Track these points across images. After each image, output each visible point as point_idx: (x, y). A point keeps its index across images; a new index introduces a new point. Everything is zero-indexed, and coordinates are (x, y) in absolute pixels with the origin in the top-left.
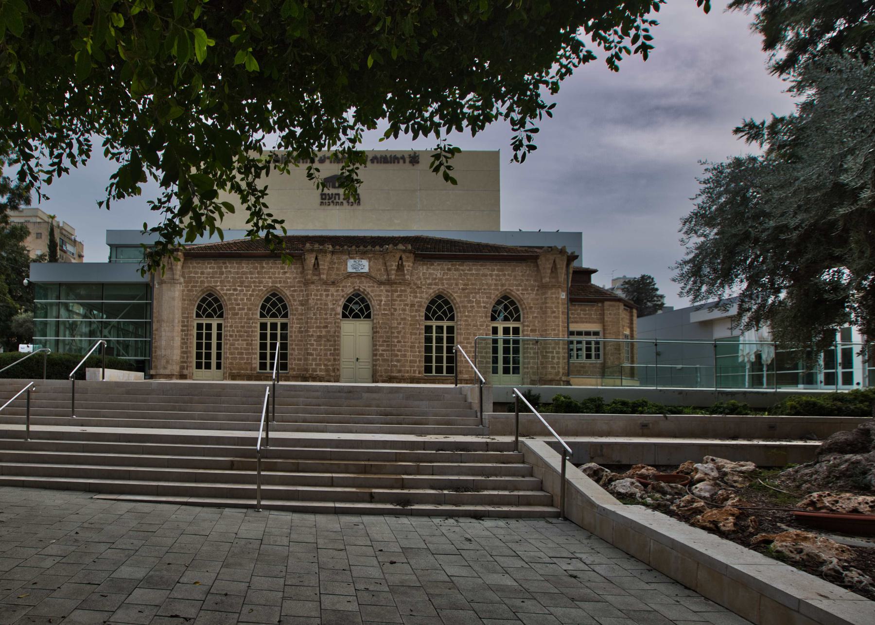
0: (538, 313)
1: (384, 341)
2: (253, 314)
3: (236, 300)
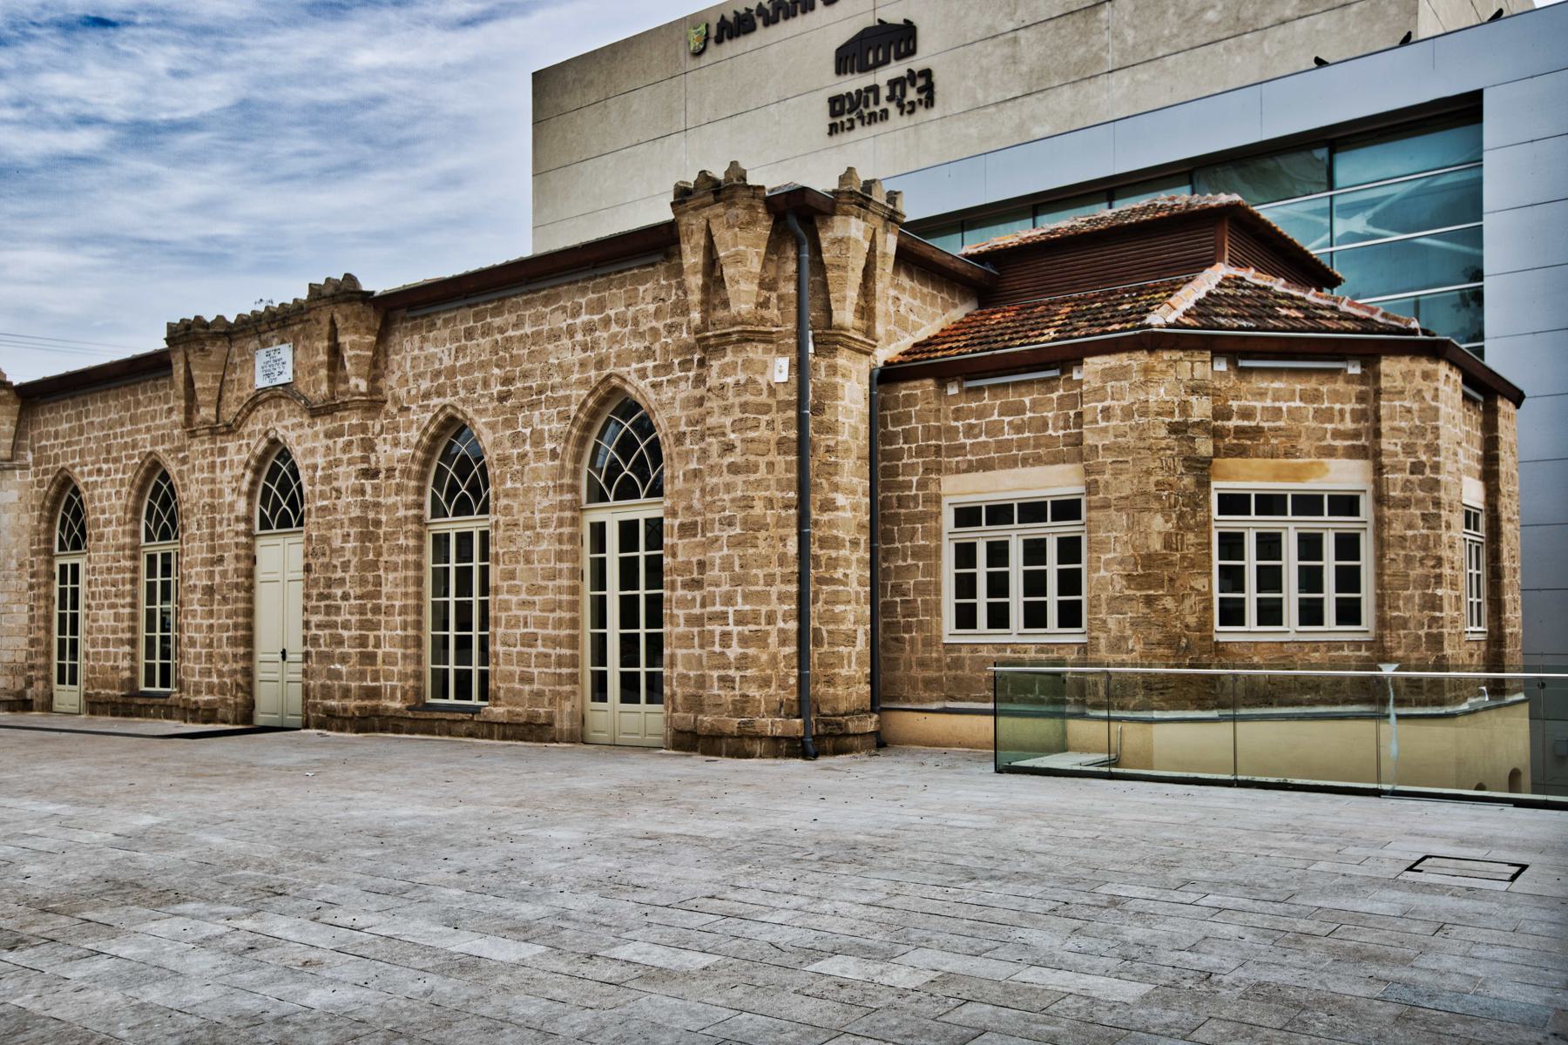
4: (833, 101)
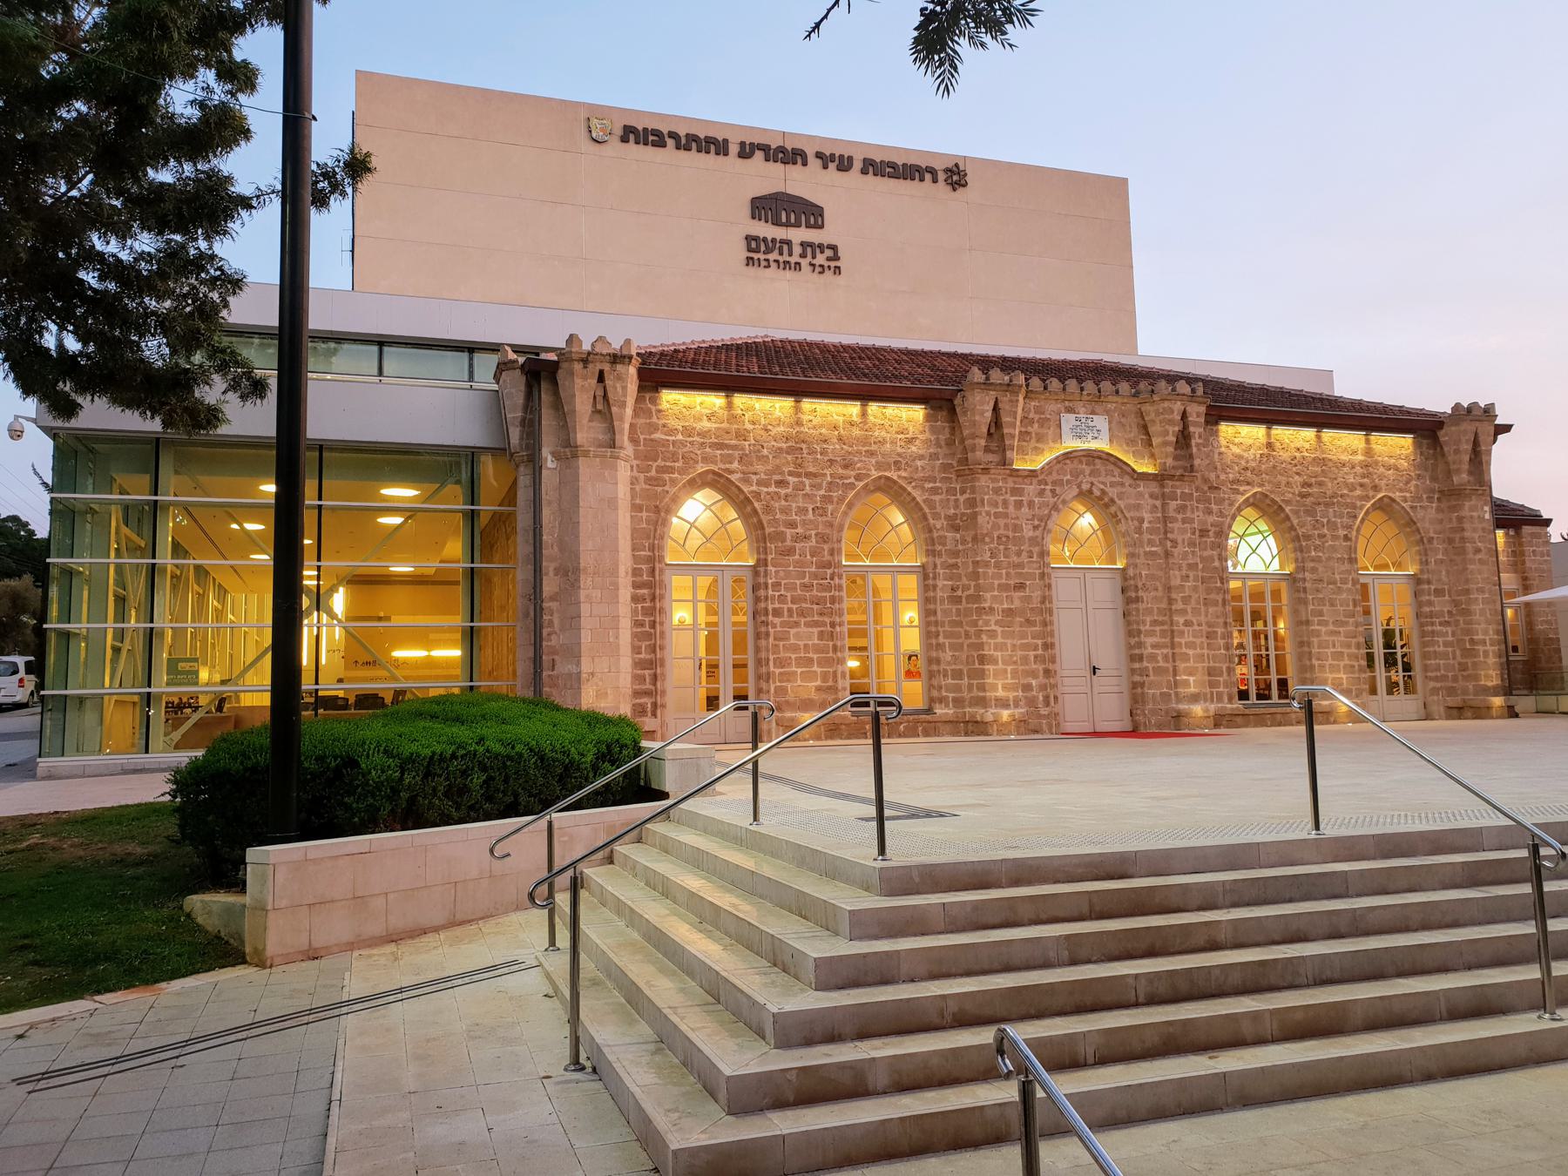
0: (1446, 552)
1: (1155, 623)
2: (832, 552)
3: (785, 511)
4: (748, 238)
